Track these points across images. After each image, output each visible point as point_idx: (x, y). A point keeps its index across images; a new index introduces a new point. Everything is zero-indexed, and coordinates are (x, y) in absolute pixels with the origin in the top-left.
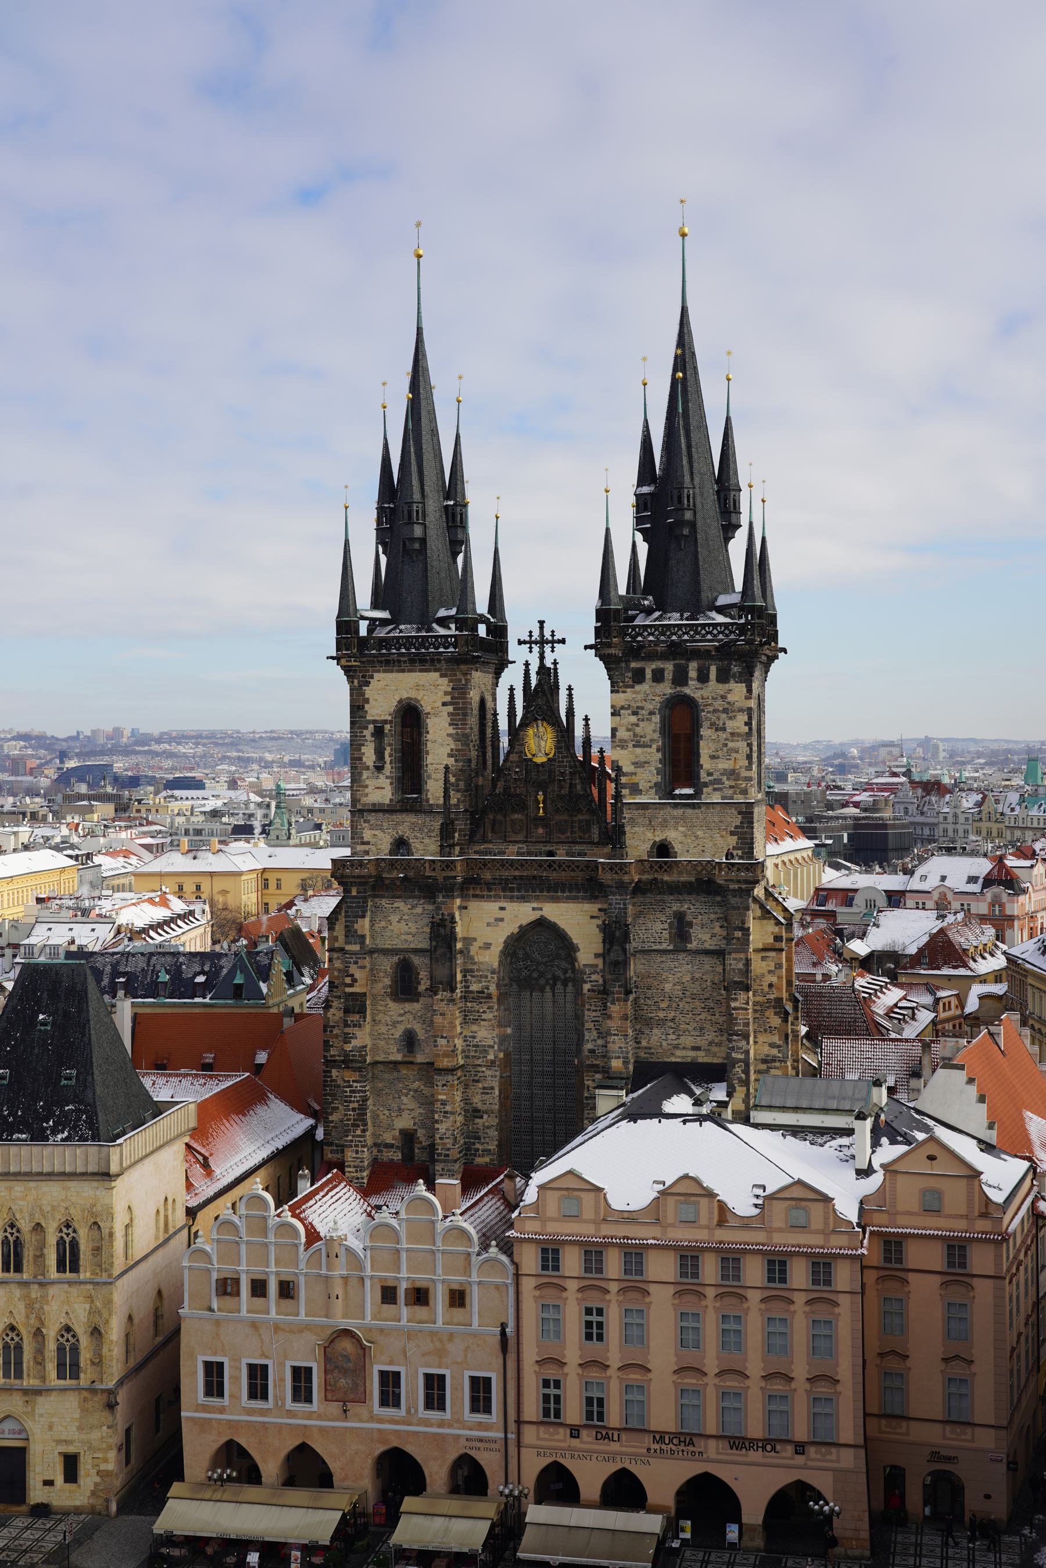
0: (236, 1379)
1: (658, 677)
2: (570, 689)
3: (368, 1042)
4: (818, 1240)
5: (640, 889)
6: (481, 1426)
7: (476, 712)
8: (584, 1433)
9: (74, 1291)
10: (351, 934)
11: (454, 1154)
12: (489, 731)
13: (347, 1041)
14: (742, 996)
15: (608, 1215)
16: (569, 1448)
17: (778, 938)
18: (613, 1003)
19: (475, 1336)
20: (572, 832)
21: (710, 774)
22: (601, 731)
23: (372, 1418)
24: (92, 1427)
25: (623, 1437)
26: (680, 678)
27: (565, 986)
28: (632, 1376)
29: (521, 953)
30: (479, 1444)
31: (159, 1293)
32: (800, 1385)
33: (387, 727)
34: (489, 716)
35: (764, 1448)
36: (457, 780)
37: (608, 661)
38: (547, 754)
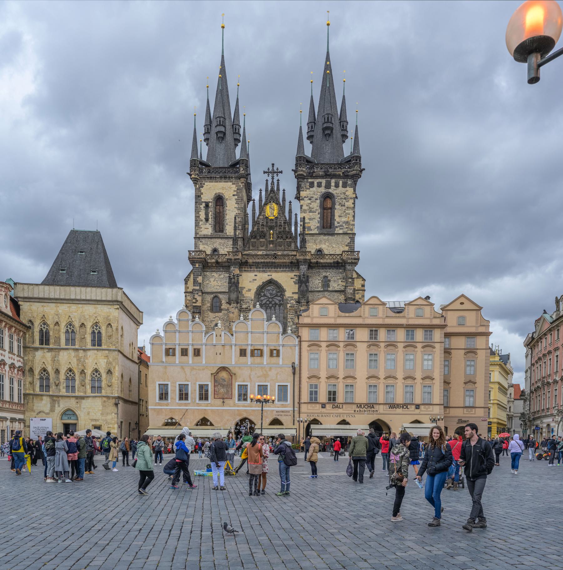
5: (311, 266)
6: (283, 406)
8: (327, 406)
9: (100, 353)
18: (302, 306)
21: (338, 223)
23: (235, 405)
25: (344, 406)
27: (280, 306)
28: (348, 381)
29: (262, 294)
30: (282, 413)
32: (419, 381)
35: (403, 407)
36: (239, 225)
38: (274, 216)
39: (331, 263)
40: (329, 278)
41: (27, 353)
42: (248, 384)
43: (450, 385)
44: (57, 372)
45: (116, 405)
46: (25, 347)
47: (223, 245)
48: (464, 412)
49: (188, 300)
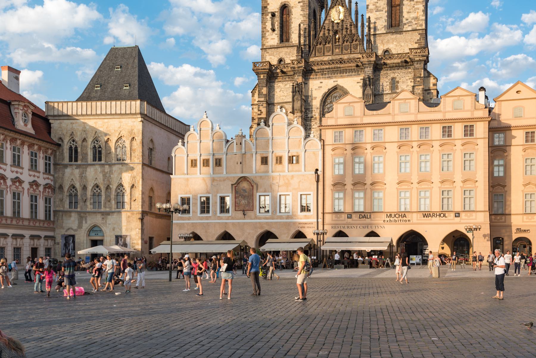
6: (306, 217)
8: (354, 216)
16: (347, 224)
19: (303, 175)
20: (351, 49)
23: (256, 218)
32: (459, 184)
35: (440, 215)
38: (340, 19)
39: (398, 63)
40: (397, 80)
41: (57, 170)
43: (506, 189)
44: (85, 188)
45: (142, 219)
46: (55, 164)
47: (289, 54)
48: (523, 219)
49: (254, 112)
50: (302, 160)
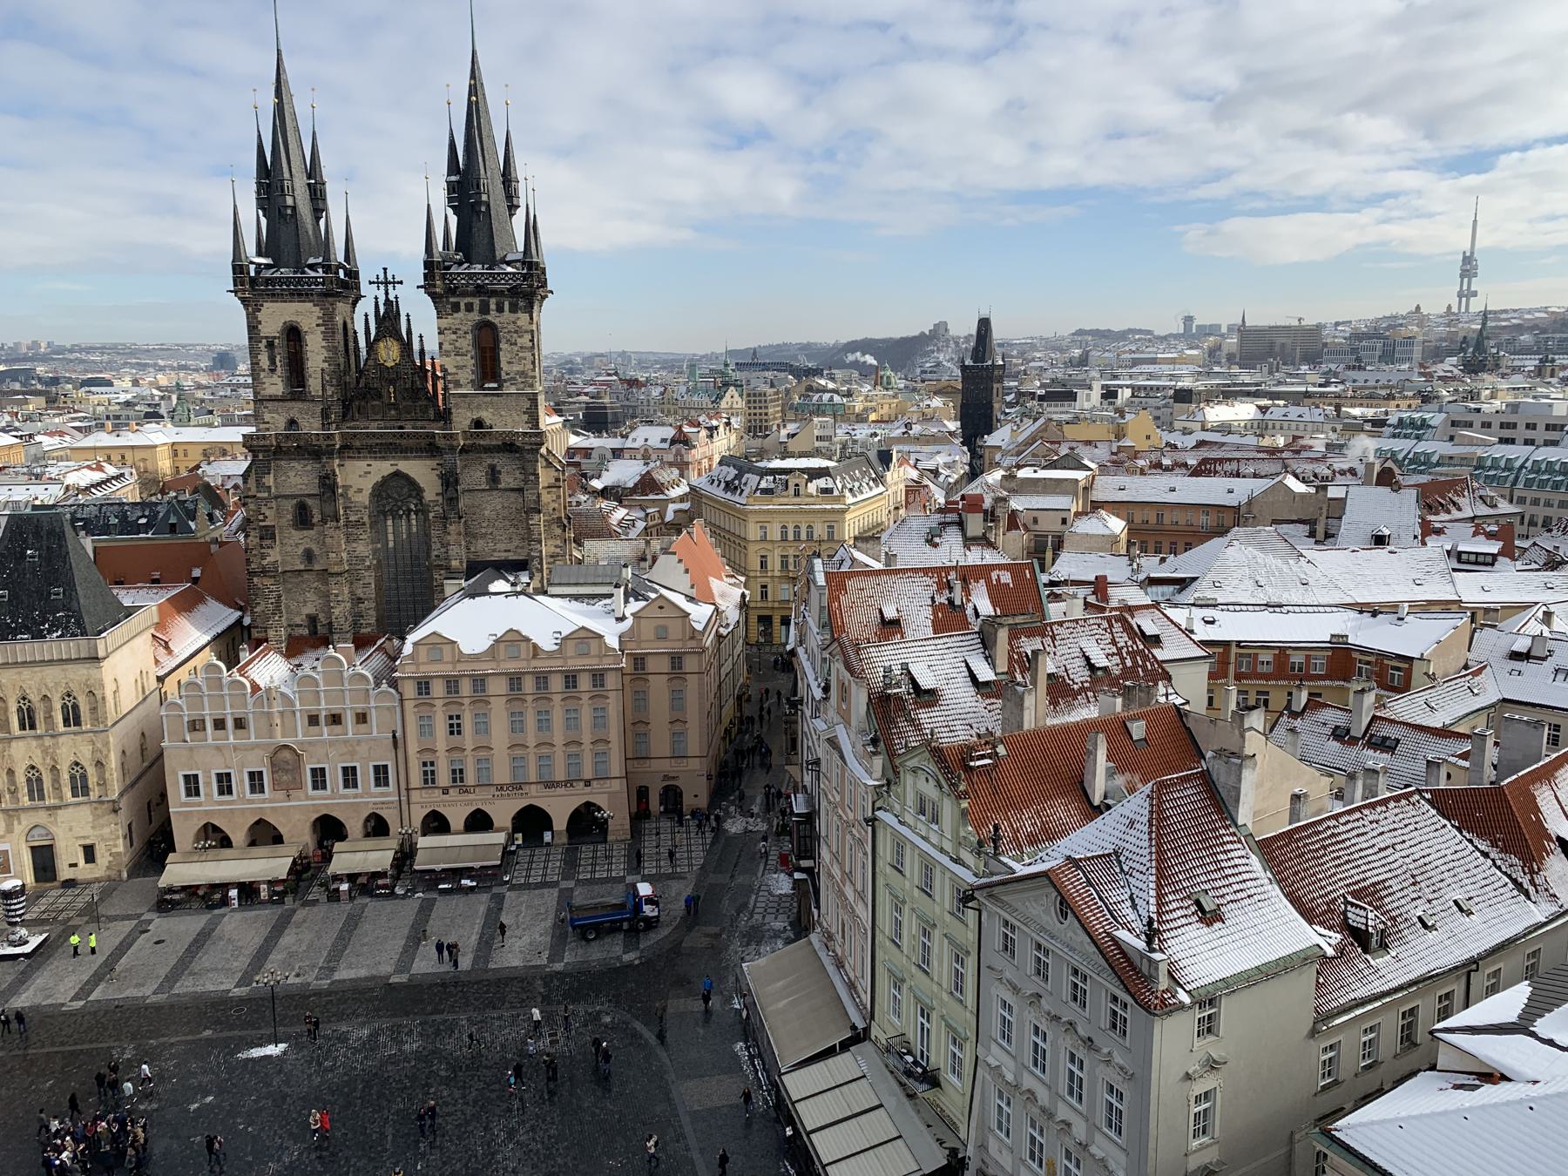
0: (208, 784)
1: (469, 308)
2: (408, 315)
3: (279, 558)
4: (594, 661)
5: (464, 450)
6: (383, 794)
7: (341, 331)
8: (451, 791)
9: (79, 738)
10: (260, 485)
11: (346, 627)
12: (351, 345)
13: (263, 557)
14: (536, 517)
15: (461, 657)
17: (557, 480)
22: (432, 345)
23: (308, 798)
24: (103, 826)
26: (485, 309)
31: (143, 734)
32: (587, 746)
33: (277, 341)
34: (350, 333)
37: (433, 296)
42: (326, 766)
50: (373, 716)
